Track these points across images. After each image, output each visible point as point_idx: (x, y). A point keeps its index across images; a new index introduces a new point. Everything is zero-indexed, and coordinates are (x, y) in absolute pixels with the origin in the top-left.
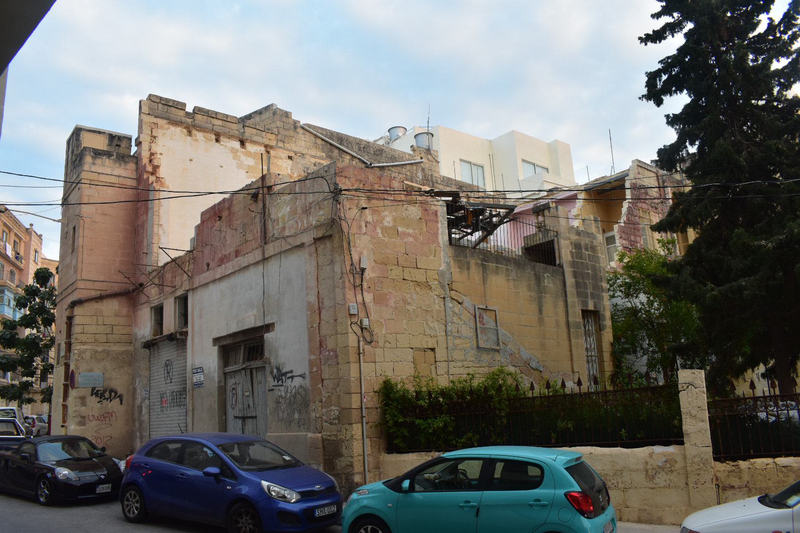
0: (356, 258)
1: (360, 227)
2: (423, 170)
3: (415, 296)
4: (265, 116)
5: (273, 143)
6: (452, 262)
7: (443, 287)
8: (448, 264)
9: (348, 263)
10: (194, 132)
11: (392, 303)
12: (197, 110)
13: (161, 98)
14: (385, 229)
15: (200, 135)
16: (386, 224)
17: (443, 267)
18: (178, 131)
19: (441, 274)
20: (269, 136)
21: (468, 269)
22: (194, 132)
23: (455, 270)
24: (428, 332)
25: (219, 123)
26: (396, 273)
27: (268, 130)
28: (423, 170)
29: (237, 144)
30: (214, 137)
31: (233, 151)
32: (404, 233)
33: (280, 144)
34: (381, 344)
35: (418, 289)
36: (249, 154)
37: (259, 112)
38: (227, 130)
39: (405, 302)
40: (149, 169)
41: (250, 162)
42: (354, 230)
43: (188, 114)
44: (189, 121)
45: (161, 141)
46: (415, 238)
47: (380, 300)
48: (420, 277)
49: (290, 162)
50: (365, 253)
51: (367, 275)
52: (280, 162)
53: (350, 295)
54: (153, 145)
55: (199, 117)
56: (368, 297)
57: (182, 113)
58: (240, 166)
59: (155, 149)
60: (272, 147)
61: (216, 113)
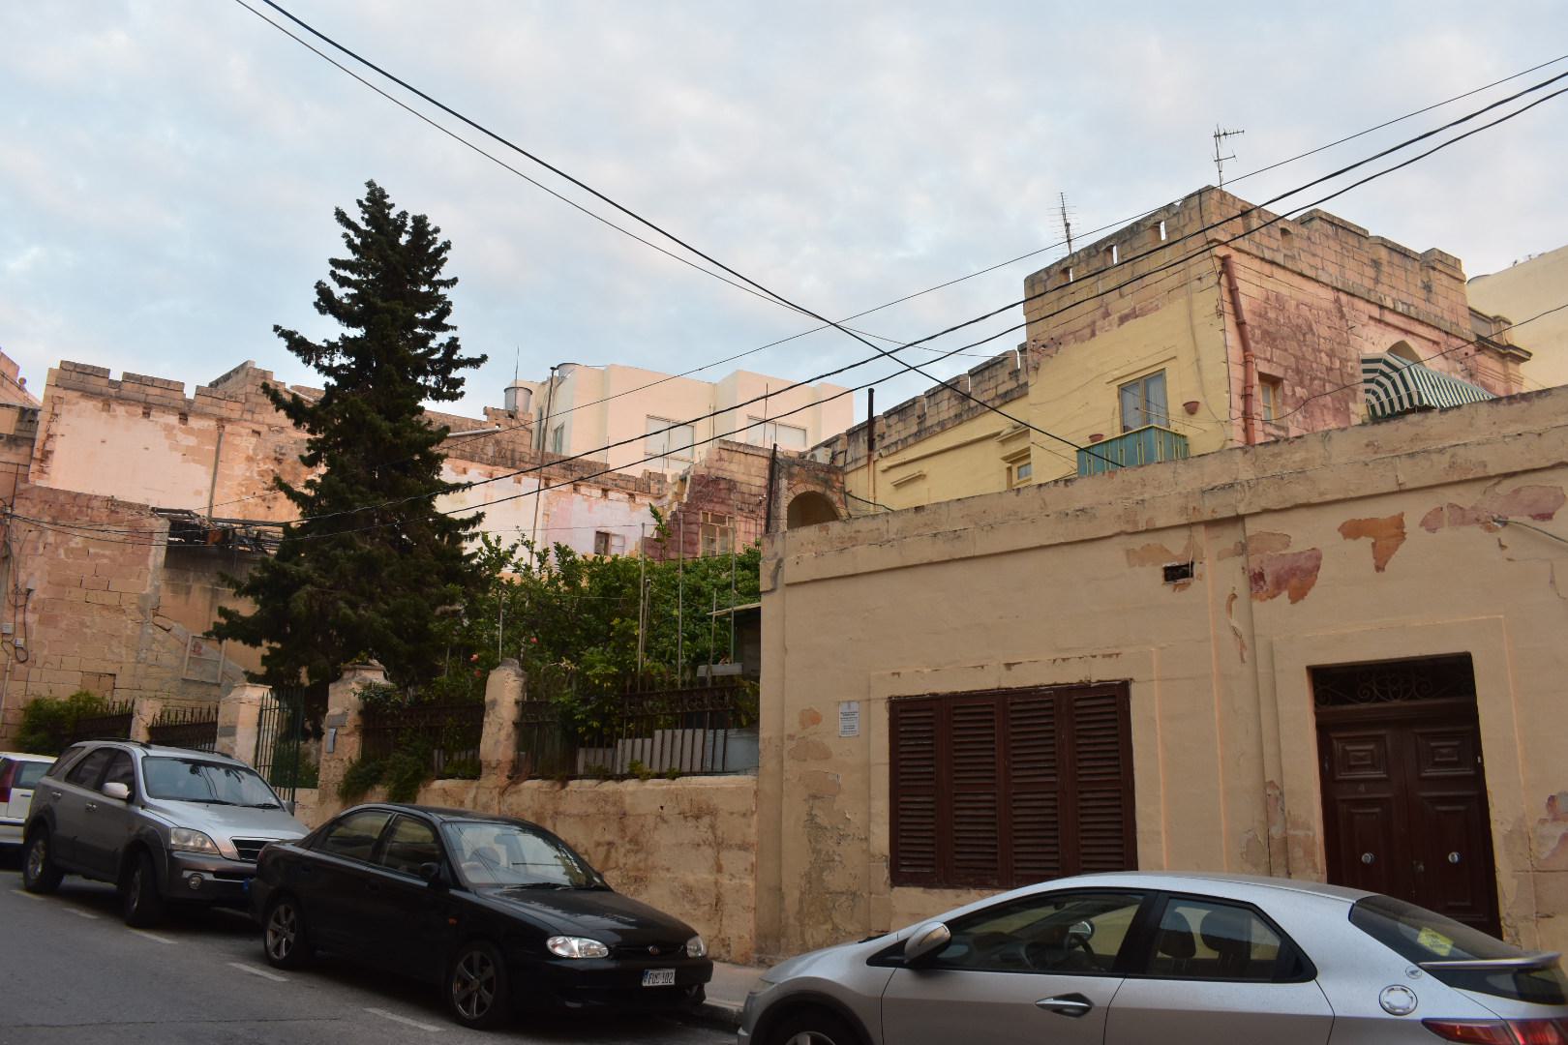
0: (22, 577)
1: (36, 549)
2: (498, 443)
3: (98, 619)
4: (242, 375)
5: (236, 415)
6: (163, 587)
7: (142, 611)
8: (157, 588)
9: (11, 586)
10: (114, 406)
11: (63, 624)
12: (127, 376)
13: (76, 365)
14: (69, 551)
15: (120, 410)
16: (72, 545)
17: (148, 590)
18: (89, 405)
19: (145, 598)
20: (232, 405)
21: (188, 593)
22: (114, 406)
23: (167, 598)
24: (109, 656)
25: (158, 391)
26: (77, 594)
27: (233, 398)
28: (498, 443)
29: (173, 419)
30: (140, 411)
31: (168, 429)
32: (97, 555)
33: (248, 416)
34: (39, 663)
35: (105, 613)
36: (191, 432)
37: (236, 371)
38: (166, 401)
39: (83, 624)
40: (37, 455)
41: (192, 441)
42: (28, 550)
43: (112, 382)
44: (112, 391)
45: (64, 419)
46: (113, 559)
47: (48, 620)
48: (111, 599)
49: (254, 440)
50: (37, 574)
51: (34, 596)
52: (237, 441)
53: (8, 614)
54: (53, 425)
55: (128, 386)
56: (31, 618)
57: (103, 382)
58: (174, 447)
59: (54, 428)
60: (229, 420)
61: (153, 380)
